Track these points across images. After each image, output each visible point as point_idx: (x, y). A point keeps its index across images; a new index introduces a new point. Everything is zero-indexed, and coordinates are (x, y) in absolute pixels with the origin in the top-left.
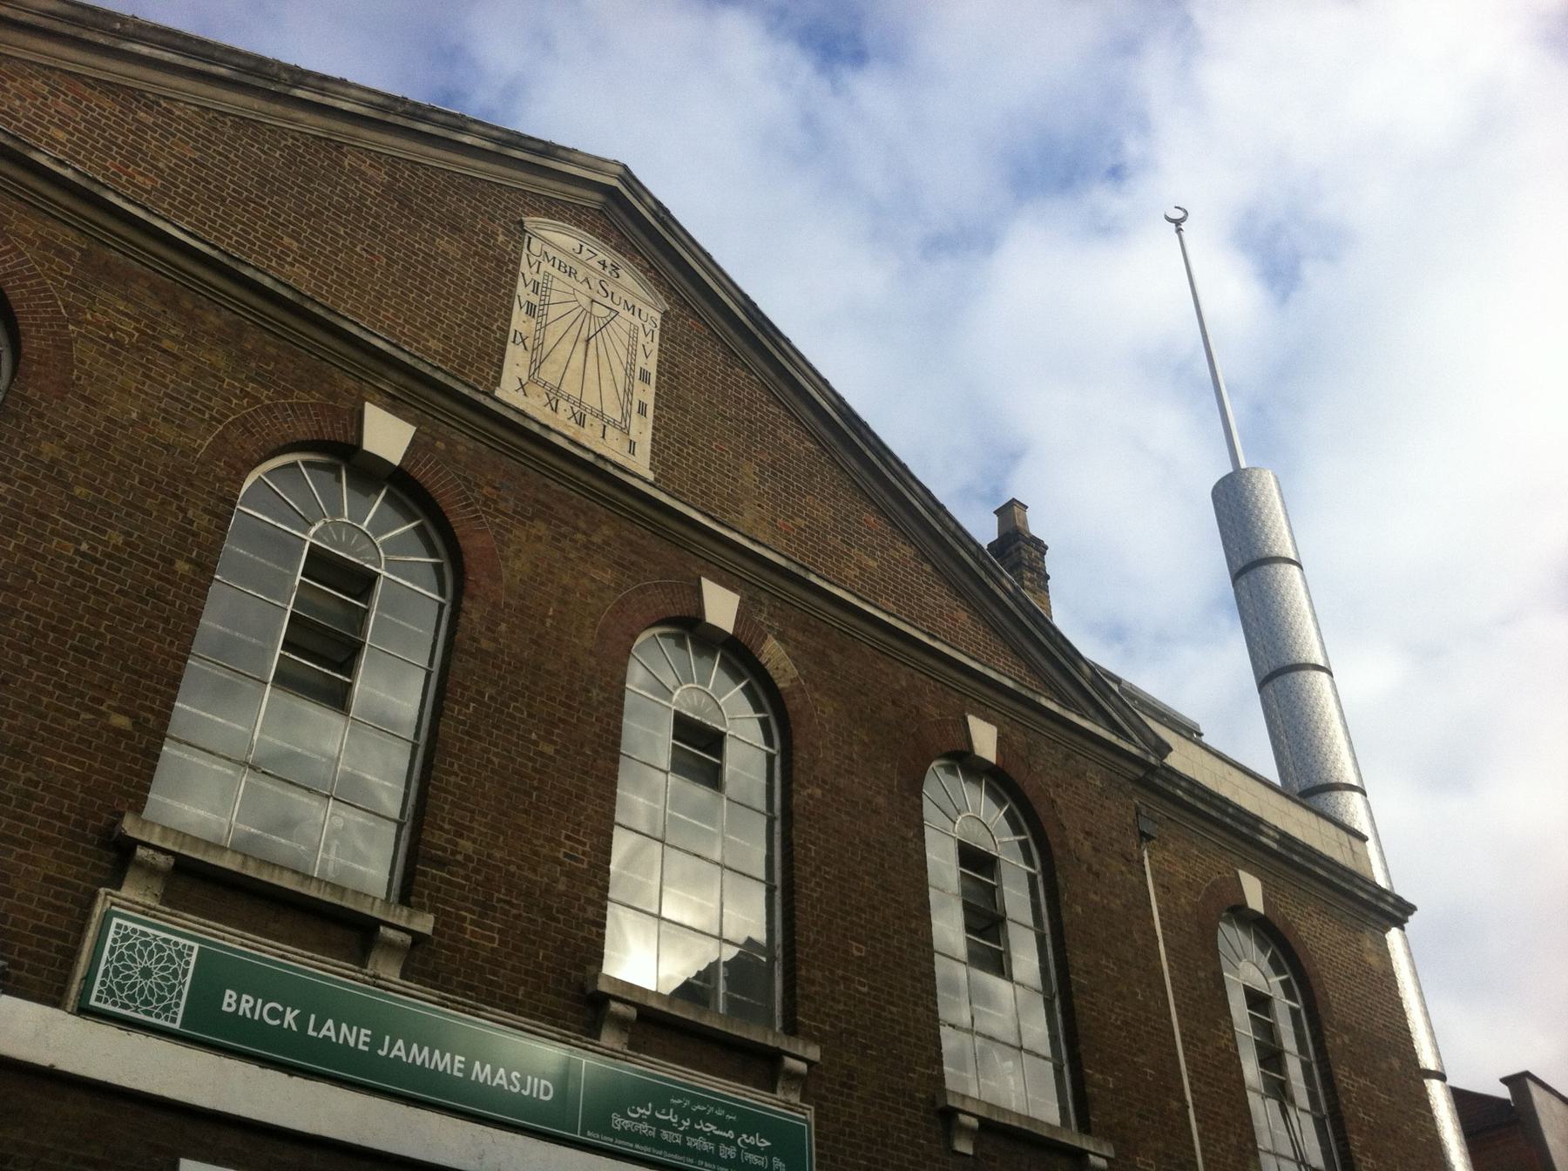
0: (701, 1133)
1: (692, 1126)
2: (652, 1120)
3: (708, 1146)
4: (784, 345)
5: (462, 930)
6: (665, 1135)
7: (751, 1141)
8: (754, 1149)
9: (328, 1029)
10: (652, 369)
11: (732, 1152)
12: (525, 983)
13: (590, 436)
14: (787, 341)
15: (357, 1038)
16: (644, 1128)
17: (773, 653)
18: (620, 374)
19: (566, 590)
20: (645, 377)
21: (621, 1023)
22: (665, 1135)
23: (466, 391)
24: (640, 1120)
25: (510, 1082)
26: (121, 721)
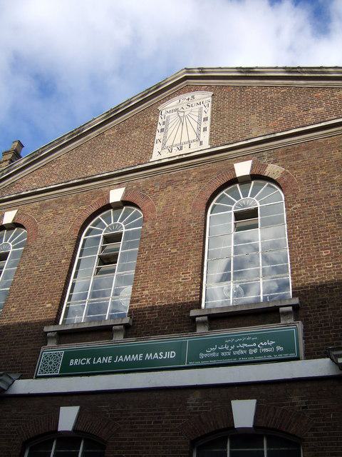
0: (240, 348)
1: (235, 347)
2: (217, 351)
3: (242, 352)
4: (256, 70)
5: (145, 317)
6: (223, 354)
7: (265, 344)
8: (267, 346)
9: (99, 360)
10: (209, 115)
11: (255, 351)
12: (167, 324)
13: (186, 150)
14: (257, 68)
15: (107, 360)
16: (214, 354)
17: (273, 170)
18: (195, 126)
19: (179, 200)
20: (206, 119)
21: (203, 323)
22: (223, 354)
23: (133, 168)
24: (212, 352)
25: (159, 356)
26: (49, 305)
